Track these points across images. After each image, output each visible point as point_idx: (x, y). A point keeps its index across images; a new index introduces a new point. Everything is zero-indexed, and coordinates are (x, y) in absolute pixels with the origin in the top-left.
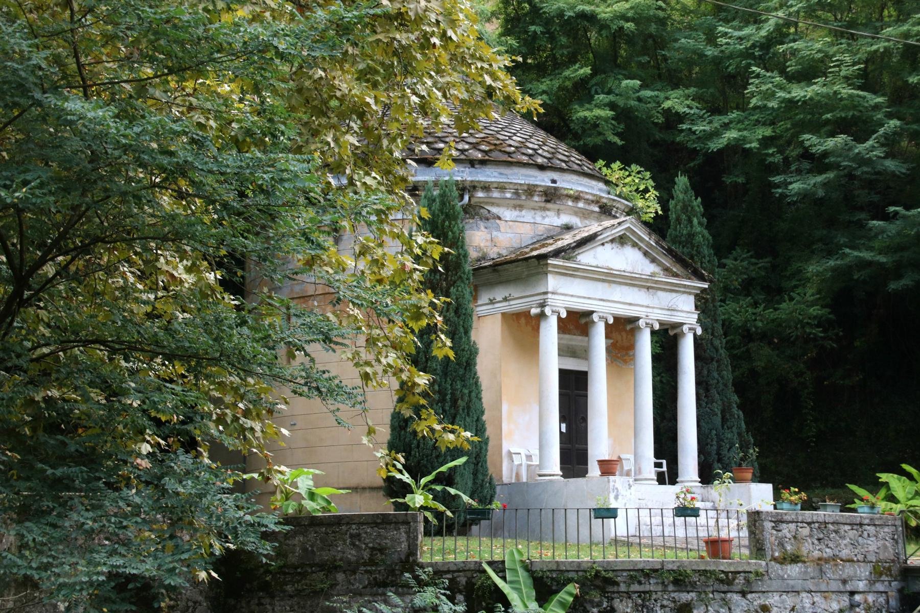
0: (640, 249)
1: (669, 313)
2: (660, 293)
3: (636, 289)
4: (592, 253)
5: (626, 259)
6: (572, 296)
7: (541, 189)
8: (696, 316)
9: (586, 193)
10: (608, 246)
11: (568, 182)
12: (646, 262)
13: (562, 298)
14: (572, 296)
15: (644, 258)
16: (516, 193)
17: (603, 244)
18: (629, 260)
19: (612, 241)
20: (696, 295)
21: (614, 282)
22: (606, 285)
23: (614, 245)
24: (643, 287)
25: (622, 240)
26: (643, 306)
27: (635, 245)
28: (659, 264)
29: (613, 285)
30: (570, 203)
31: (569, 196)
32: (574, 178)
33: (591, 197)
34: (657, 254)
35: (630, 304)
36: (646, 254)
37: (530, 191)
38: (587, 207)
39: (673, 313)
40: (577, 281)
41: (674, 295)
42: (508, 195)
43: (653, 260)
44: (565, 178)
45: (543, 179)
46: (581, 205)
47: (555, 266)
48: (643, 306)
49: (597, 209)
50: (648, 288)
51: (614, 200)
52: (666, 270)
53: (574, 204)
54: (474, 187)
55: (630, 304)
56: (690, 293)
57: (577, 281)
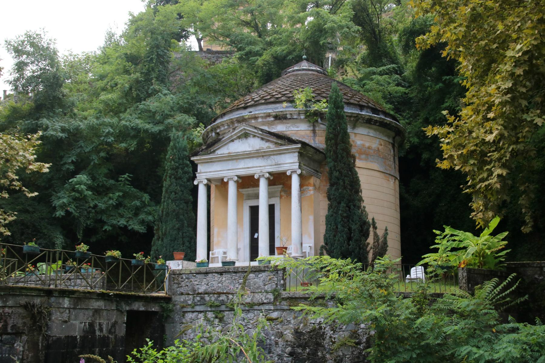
0: (258, 137)
1: (277, 166)
2: (272, 157)
3: (255, 159)
4: (226, 147)
5: (249, 145)
6: (210, 172)
7: (235, 120)
8: (298, 164)
9: (260, 114)
10: (236, 142)
11: (262, 110)
12: (264, 142)
13: (205, 174)
14: (210, 172)
15: (261, 141)
16: (228, 125)
17: (233, 141)
18: (254, 144)
19: (239, 138)
20: (299, 152)
21: (239, 159)
22: (235, 161)
23: (240, 140)
24: (260, 156)
25: (246, 135)
26: (257, 167)
27: (254, 136)
28: (272, 142)
29: (239, 161)
30: (253, 121)
31: (249, 118)
32: (263, 107)
33: (263, 115)
34: (267, 136)
35: (248, 168)
36: (262, 139)
37: (232, 122)
38: (264, 120)
39: (279, 166)
40: (216, 163)
41: (283, 156)
42: (226, 127)
43: (268, 141)
44: (257, 109)
45: (245, 113)
46: (260, 120)
47: (197, 160)
48: (257, 167)
49: (273, 119)
50: (263, 156)
51: (282, 111)
52: (276, 143)
53: (256, 121)
54: (216, 129)
55: (248, 168)
56: (294, 152)
57: (215, 164)
